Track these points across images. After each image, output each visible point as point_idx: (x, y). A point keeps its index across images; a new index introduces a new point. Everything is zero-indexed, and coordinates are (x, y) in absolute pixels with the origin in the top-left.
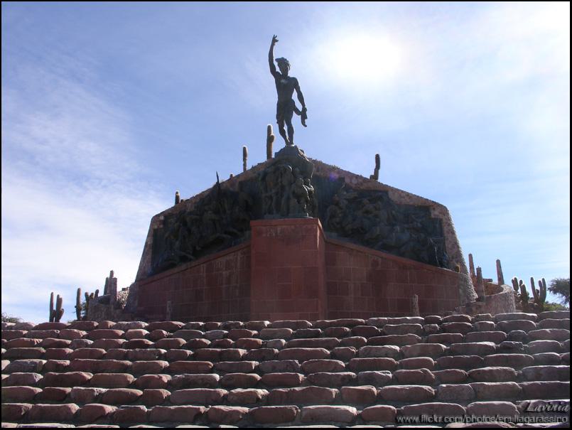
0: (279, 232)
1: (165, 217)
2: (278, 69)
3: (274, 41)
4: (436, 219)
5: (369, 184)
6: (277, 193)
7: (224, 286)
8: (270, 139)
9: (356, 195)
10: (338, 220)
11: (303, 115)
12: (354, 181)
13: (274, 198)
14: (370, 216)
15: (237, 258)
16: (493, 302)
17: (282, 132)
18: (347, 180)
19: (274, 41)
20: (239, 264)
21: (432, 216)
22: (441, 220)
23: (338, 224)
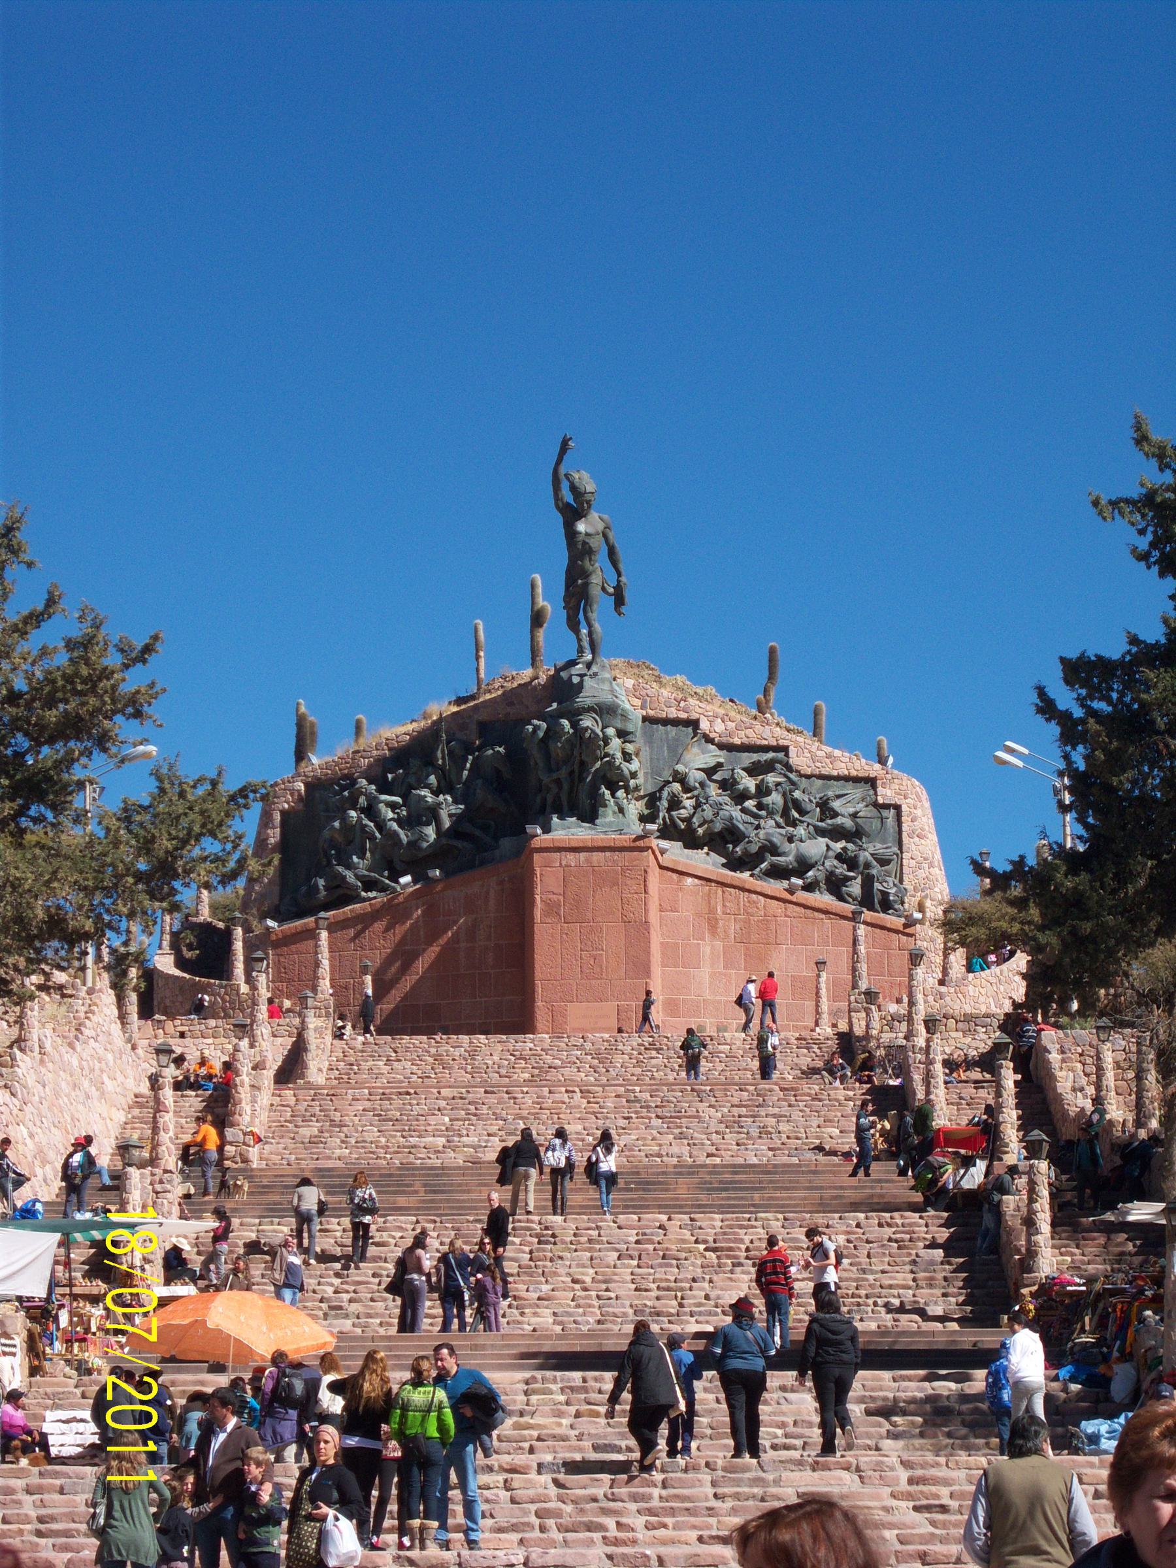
0: (582, 859)
1: (306, 784)
2: (568, 497)
3: (564, 446)
4: (886, 806)
5: (750, 732)
6: (571, 773)
7: (463, 945)
8: (537, 619)
9: (722, 760)
10: (684, 813)
11: (619, 601)
12: (719, 727)
13: (566, 786)
14: (750, 804)
15: (487, 893)
16: (971, 988)
17: (574, 626)
18: (704, 725)
19: (564, 446)
20: (492, 902)
21: (880, 800)
22: (898, 808)
23: (683, 820)
